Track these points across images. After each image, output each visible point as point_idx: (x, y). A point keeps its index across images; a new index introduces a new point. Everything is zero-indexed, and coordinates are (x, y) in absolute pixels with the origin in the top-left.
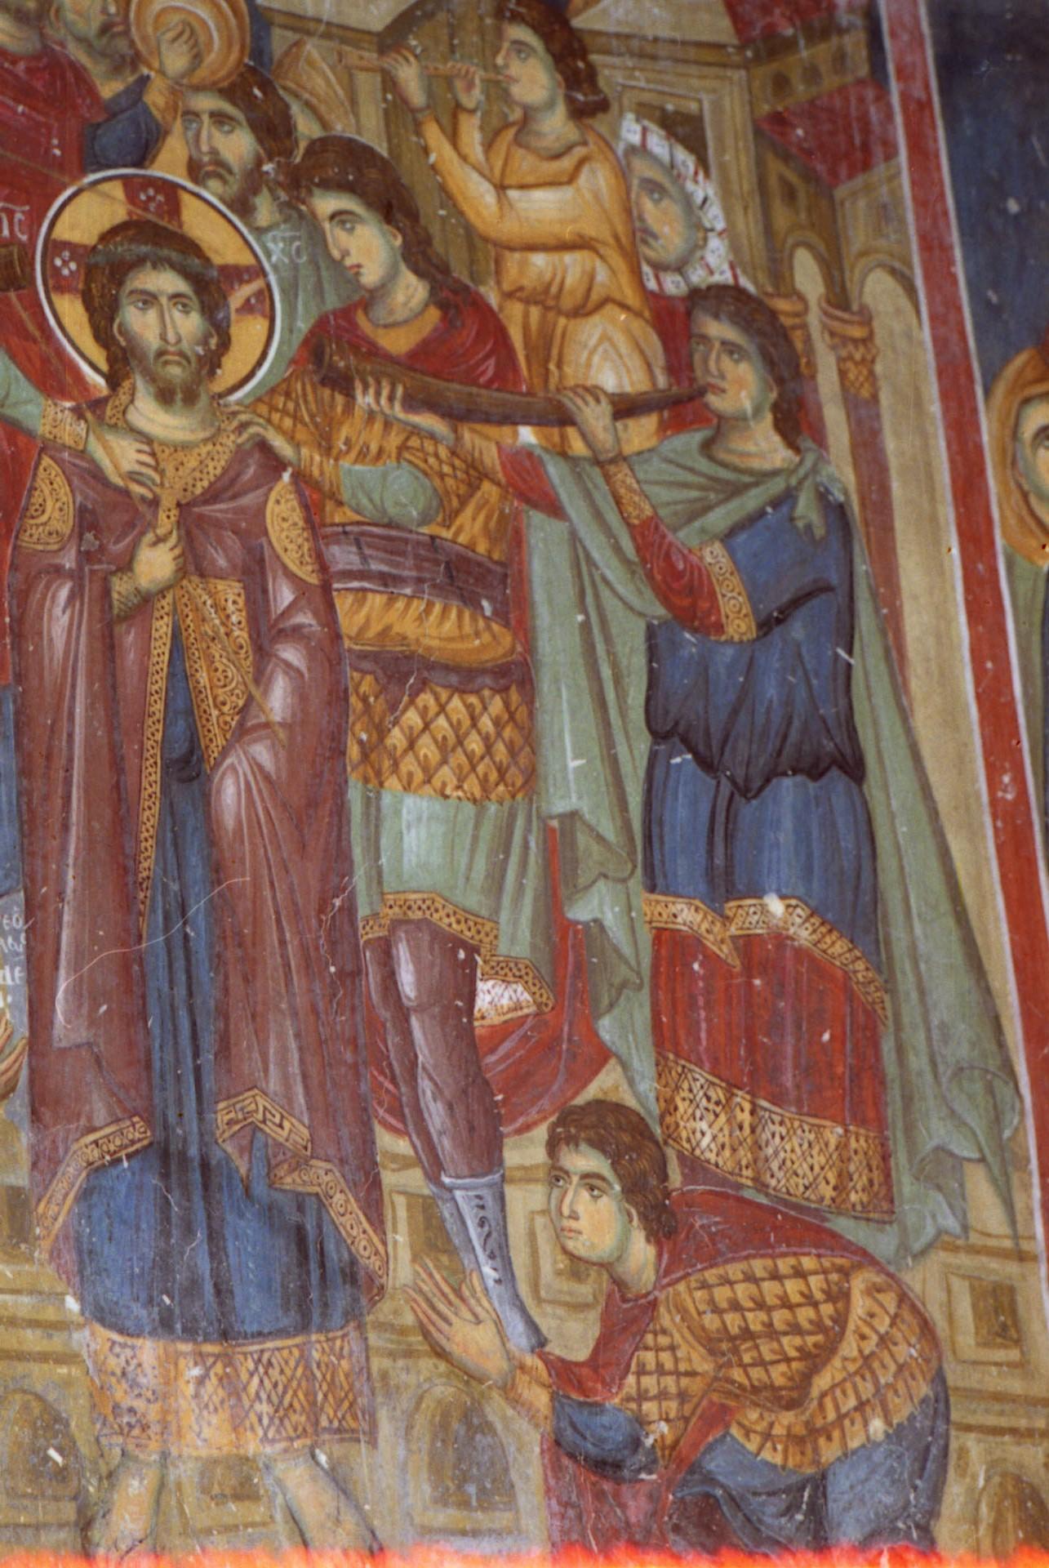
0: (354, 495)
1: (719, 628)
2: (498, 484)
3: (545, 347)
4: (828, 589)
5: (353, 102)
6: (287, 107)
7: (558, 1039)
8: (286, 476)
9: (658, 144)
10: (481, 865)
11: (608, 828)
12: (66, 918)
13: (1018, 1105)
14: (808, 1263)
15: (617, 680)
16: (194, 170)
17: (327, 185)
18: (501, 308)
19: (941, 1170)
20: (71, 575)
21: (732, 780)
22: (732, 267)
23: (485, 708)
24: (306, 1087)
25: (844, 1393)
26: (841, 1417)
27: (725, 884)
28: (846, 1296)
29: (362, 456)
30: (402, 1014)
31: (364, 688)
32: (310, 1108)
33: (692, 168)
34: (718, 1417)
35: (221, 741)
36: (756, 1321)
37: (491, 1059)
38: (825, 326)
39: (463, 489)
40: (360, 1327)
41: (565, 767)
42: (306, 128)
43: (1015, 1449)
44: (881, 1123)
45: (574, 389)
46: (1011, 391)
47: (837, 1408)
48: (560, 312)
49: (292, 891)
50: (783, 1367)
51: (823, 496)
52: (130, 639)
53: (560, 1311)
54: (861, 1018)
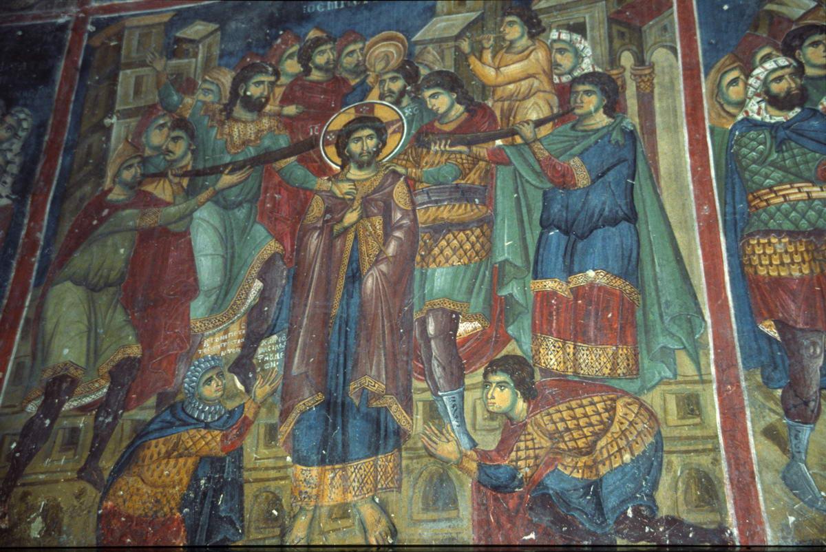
0: (427, 178)
1: (575, 185)
2: (486, 161)
3: (508, 114)
4: (625, 160)
5: (443, 58)
6: (417, 68)
7: (491, 338)
8: (402, 179)
9: (565, 36)
10: (465, 285)
11: (519, 262)
12: (302, 334)
13: (703, 324)
14: (596, 399)
15: (529, 211)
16: (382, 97)
17: (429, 88)
18: (493, 106)
19: (667, 355)
20: (320, 228)
21: (576, 235)
22: (593, 66)
23: (473, 233)
24: (386, 373)
25: (612, 446)
26: (610, 456)
27: (570, 271)
28: (614, 409)
29: (432, 166)
30: (427, 340)
31: (426, 238)
32: (387, 378)
33: (579, 39)
34: (551, 463)
35: (368, 266)
36: (571, 424)
37: (462, 349)
38: (632, 74)
39: (471, 166)
40: (400, 450)
41: (503, 246)
42: (424, 72)
43: (697, 458)
44: (635, 343)
45: (519, 123)
46: (718, 71)
47: (608, 452)
48: (517, 100)
49: (389, 308)
50: (584, 440)
51: (623, 131)
52: (338, 243)
53: (484, 433)
54: (627, 305)
